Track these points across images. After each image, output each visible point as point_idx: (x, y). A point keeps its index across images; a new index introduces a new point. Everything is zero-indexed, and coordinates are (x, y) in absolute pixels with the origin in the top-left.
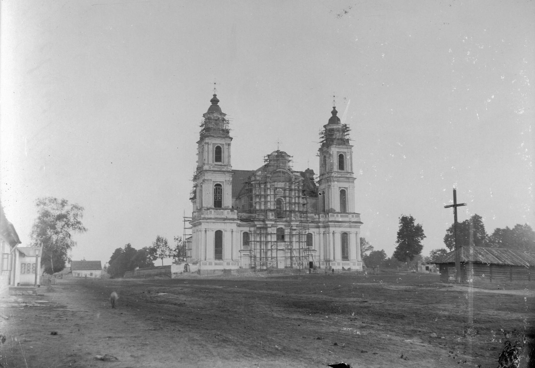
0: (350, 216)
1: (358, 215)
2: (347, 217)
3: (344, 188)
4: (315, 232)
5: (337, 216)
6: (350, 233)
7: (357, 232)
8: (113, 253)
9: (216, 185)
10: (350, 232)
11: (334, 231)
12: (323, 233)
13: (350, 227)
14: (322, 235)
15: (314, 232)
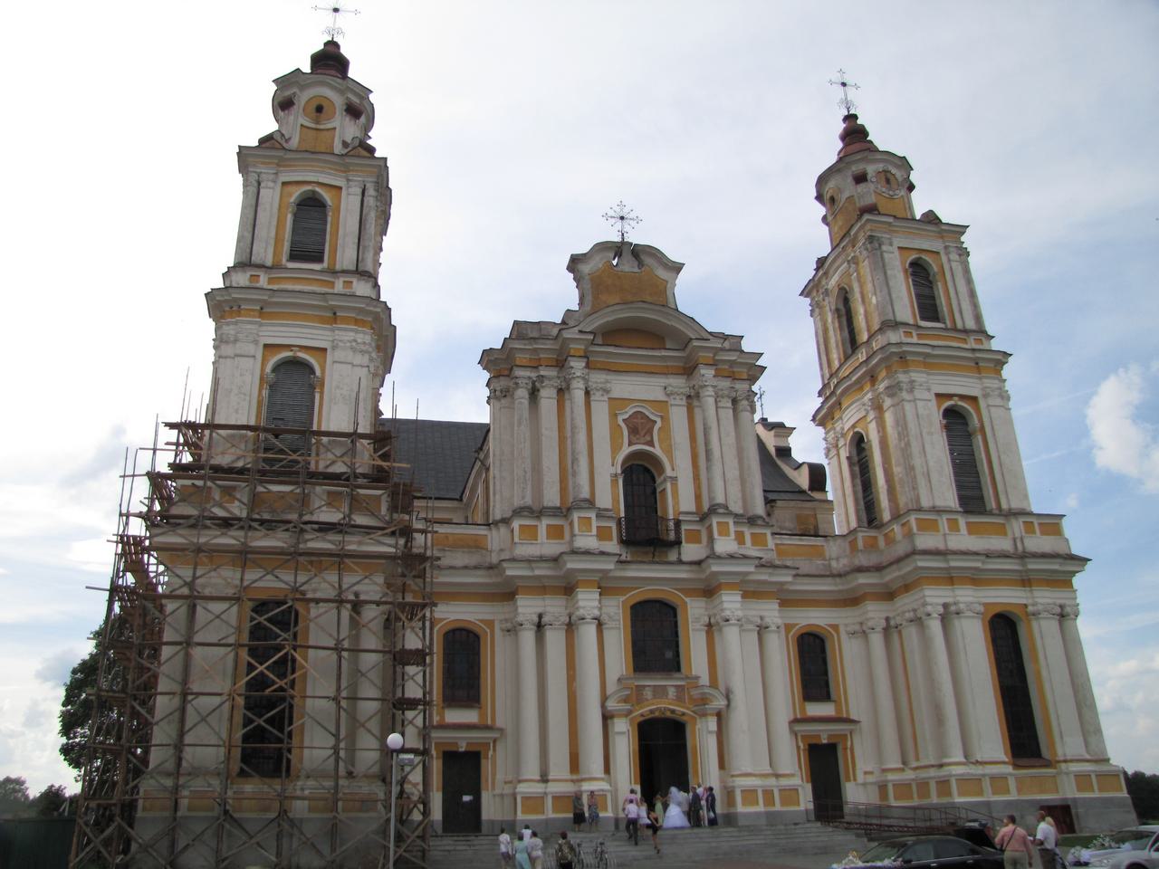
0: (1017, 526)
1: (1052, 524)
2: (1001, 530)
3: (962, 397)
4: (842, 629)
5: (954, 526)
6: (1027, 614)
7: (1062, 607)
8: (65, 760)
9: (277, 368)
10: (1030, 609)
11: (945, 606)
12: (883, 623)
13: (1026, 581)
14: (877, 640)
15: (835, 627)
